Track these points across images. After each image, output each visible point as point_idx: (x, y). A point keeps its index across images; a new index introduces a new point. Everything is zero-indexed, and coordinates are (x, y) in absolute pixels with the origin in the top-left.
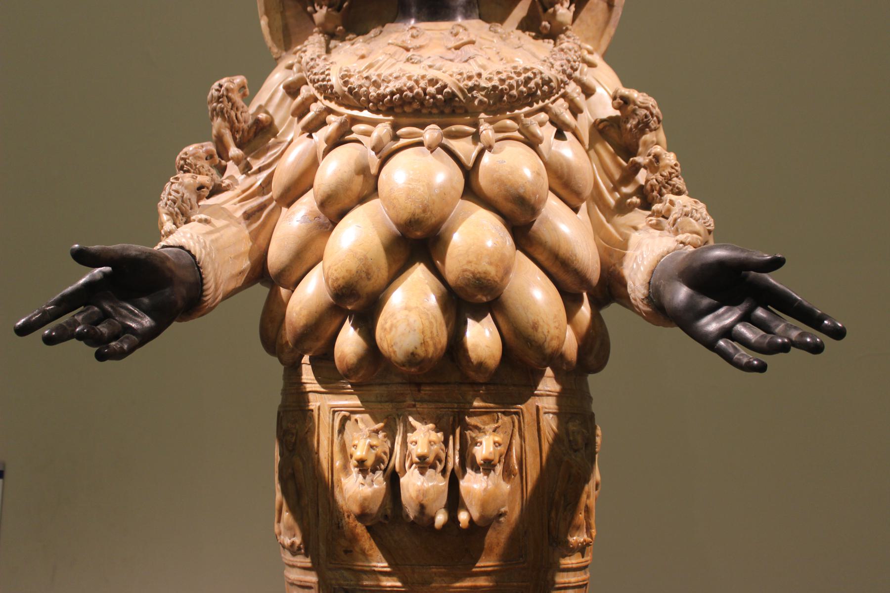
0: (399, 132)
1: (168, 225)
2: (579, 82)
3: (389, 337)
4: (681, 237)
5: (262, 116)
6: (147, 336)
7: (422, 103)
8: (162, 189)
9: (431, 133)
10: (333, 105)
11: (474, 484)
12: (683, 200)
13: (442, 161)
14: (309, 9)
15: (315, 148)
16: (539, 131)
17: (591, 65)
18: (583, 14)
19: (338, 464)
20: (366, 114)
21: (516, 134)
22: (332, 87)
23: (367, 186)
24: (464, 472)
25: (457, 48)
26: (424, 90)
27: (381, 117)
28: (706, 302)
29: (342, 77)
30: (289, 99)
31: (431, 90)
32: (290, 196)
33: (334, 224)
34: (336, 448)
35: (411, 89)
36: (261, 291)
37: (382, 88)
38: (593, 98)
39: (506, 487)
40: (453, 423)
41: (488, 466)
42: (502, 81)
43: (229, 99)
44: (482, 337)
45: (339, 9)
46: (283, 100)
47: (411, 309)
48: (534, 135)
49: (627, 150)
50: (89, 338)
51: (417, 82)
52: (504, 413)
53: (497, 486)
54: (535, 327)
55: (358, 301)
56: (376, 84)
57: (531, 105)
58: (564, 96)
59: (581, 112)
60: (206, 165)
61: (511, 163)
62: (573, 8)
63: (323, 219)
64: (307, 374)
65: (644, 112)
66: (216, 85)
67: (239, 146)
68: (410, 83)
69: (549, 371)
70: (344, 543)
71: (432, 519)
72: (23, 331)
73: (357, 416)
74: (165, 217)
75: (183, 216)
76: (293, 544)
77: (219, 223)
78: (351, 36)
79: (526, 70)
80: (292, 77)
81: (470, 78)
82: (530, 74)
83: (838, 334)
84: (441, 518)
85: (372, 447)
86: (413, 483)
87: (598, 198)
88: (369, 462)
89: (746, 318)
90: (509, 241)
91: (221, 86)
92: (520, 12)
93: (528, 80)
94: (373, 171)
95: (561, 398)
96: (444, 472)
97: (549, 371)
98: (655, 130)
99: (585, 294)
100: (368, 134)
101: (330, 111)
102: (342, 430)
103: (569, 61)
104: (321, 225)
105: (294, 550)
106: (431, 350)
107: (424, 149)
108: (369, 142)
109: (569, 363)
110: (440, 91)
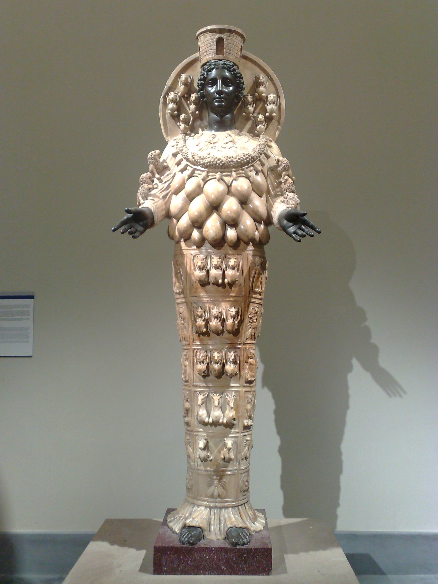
0: (209, 174)
1: (142, 201)
2: (265, 154)
3: (207, 233)
4: (288, 206)
5: (165, 164)
6: (142, 233)
7: (216, 165)
8: (138, 189)
9: (218, 175)
10: (189, 164)
11: (229, 272)
12: (291, 195)
13: (221, 183)
14: (178, 124)
15: (184, 178)
16: (250, 174)
17: (270, 147)
18: (270, 126)
19: (193, 268)
20: (199, 168)
21: (243, 175)
22: (189, 159)
23: (199, 190)
24: (226, 270)
25: (227, 143)
26: (216, 162)
27: (203, 169)
28: (291, 224)
29: (192, 156)
30: (173, 158)
31: (219, 162)
32: (176, 192)
33: (191, 202)
34: (192, 264)
35: (213, 162)
36: (167, 220)
37: (204, 160)
38: (269, 159)
39: (238, 274)
40: (225, 258)
41: (233, 268)
42: (239, 159)
43: (155, 159)
44: (231, 233)
45: (188, 125)
46: (172, 158)
47: (212, 225)
48: (248, 175)
49: (279, 176)
50: (130, 233)
51: (214, 159)
52: (238, 255)
53: (235, 273)
54: (246, 231)
55: (198, 223)
56: (203, 159)
57: (248, 165)
58: (260, 160)
59: (264, 165)
60: (149, 180)
61: (242, 184)
62: (266, 125)
63: (187, 200)
64: (183, 244)
65: (283, 165)
66: (150, 154)
67: (158, 174)
68: (212, 160)
69: (251, 243)
70: (194, 290)
71: (218, 282)
72: (114, 231)
73: (198, 255)
74: (140, 198)
75: (145, 198)
76: (179, 292)
77: (156, 200)
78: (193, 134)
79: (247, 155)
80: (174, 151)
81: (230, 158)
82: (247, 156)
83: (319, 232)
84: (220, 281)
85: (202, 263)
86: (213, 272)
87: (268, 192)
88: (202, 267)
89: (300, 228)
90: (240, 207)
91: (152, 154)
92: (249, 125)
93: (247, 158)
94: (202, 186)
95: (254, 251)
96: (221, 270)
97: (251, 243)
98: (287, 170)
99: (263, 222)
100: (201, 175)
101: (187, 165)
102: (193, 260)
103: (261, 149)
104: (186, 202)
105: (179, 294)
106: (218, 237)
107: (216, 180)
108: (201, 177)
109: (256, 241)
110: (221, 162)
